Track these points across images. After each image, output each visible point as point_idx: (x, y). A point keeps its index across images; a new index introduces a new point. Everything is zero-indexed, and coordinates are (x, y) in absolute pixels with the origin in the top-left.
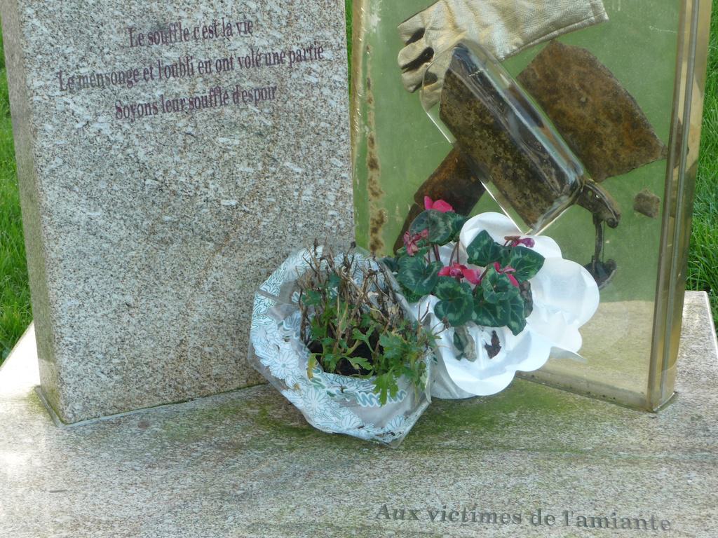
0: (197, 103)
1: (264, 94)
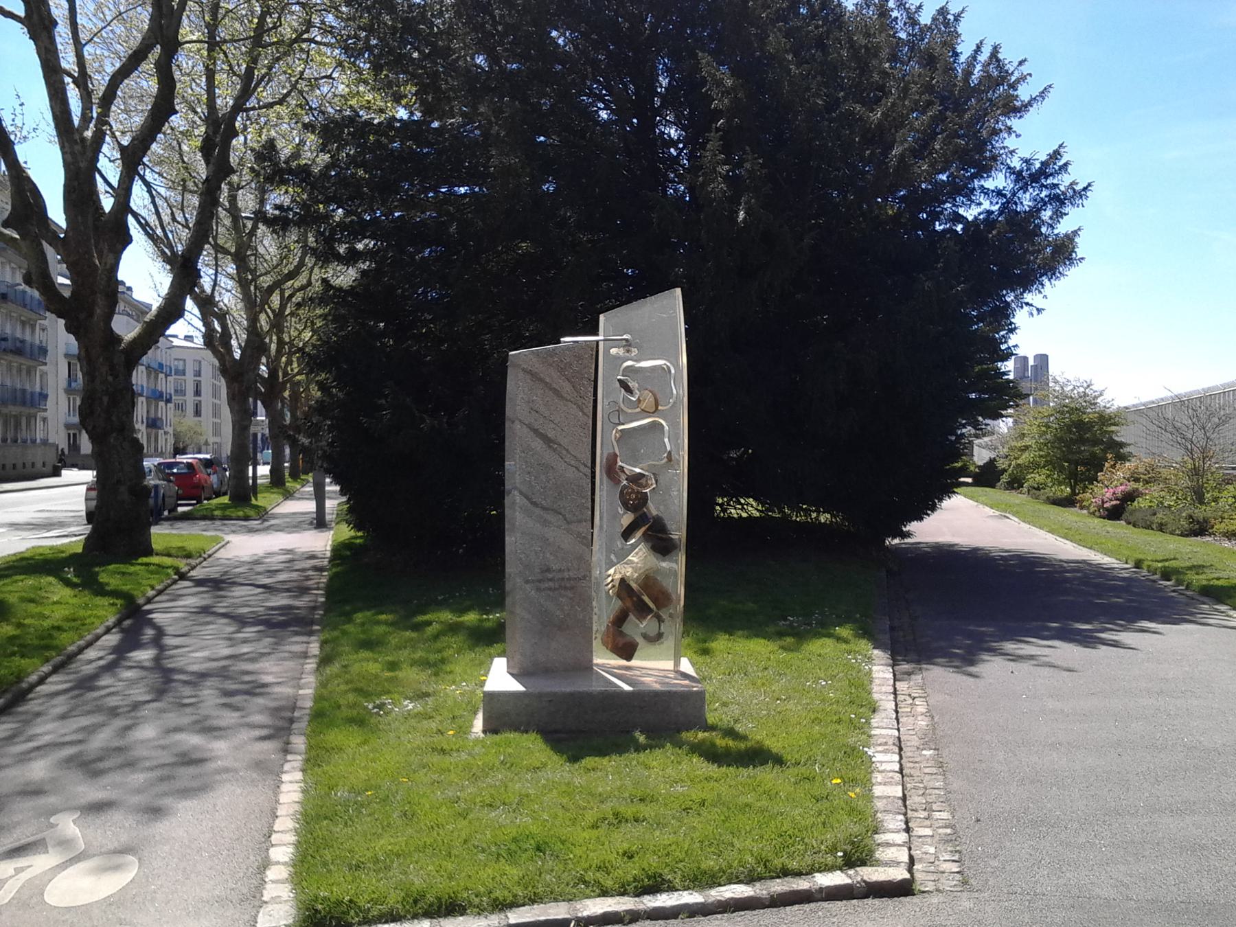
0: (555, 589)
1: (572, 588)
